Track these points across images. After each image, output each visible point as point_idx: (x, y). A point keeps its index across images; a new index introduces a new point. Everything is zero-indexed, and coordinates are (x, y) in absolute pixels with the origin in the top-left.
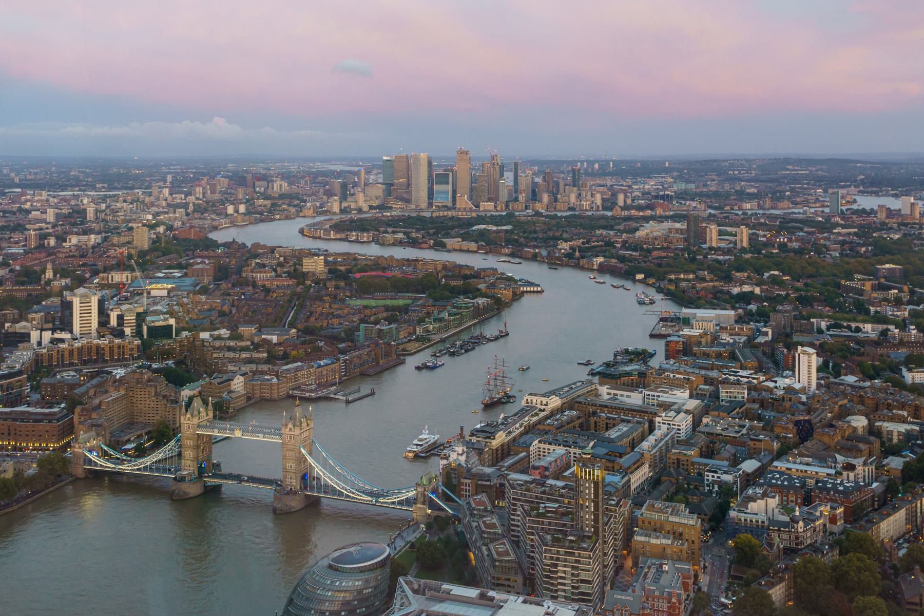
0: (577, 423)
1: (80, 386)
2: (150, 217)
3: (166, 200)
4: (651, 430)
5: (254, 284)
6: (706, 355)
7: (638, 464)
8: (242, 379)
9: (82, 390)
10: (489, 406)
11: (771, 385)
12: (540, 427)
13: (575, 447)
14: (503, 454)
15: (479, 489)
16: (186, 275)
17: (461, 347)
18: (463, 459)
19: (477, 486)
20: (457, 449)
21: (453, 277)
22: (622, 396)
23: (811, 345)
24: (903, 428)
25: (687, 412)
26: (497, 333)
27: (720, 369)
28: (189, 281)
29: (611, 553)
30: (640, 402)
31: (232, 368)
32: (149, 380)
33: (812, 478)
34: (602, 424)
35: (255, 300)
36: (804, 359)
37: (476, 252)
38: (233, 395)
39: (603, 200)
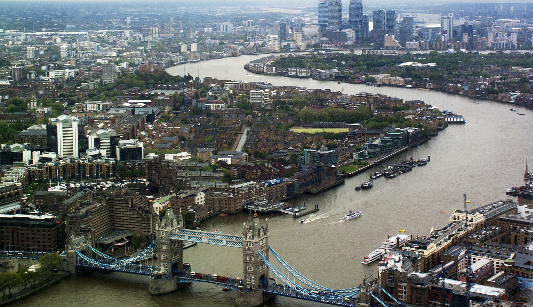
1: (68, 198)
8: (203, 195)
9: (70, 201)
13: (498, 258)
14: (433, 262)
34: (521, 238)
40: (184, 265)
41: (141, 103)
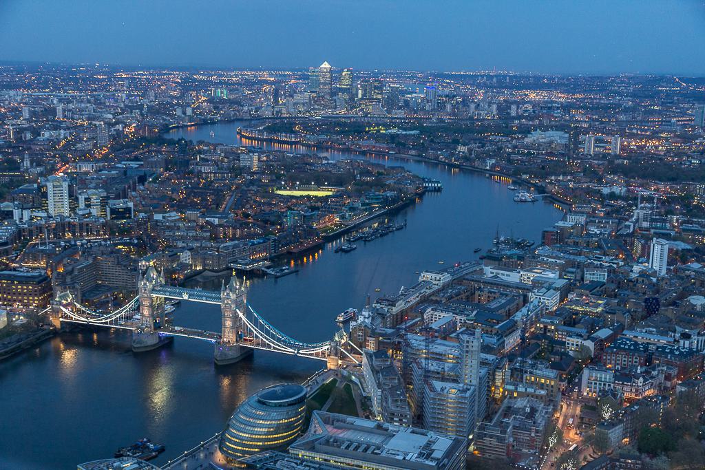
6: (576, 244)
7: (511, 328)
20: (364, 313)
22: (503, 275)
25: (556, 289)
33: (654, 344)
41: (134, 165)
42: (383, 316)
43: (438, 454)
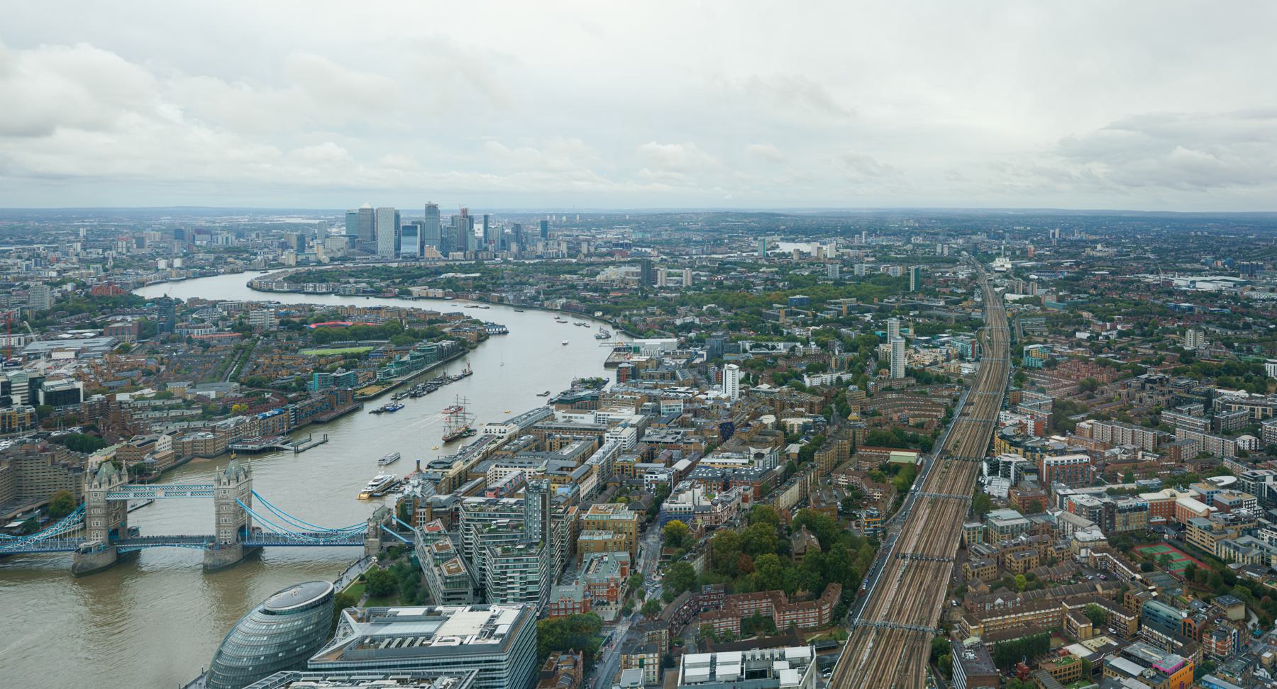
0: (533, 446)
2: (54, 274)
3: (77, 255)
4: (601, 444)
5: (190, 341)
7: (587, 475)
8: (169, 438)
10: (449, 441)
11: (703, 397)
12: (498, 453)
15: (434, 515)
16: (101, 334)
17: (424, 389)
18: (418, 490)
19: (432, 513)
21: (418, 322)
23: (736, 363)
24: (801, 421)
25: (632, 426)
26: (461, 373)
27: (662, 387)
28: (104, 340)
29: (558, 554)
30: (592, 422)
31: (157, 428)
32: (44, 450)
34: (556, 444)
35: (191, 356)
36: (729, 373)
37: (442, 299)
38: (157, 456)
39: (569, 248)
40: (129, 530)
42: (436, 482)
43: (502, 630)
